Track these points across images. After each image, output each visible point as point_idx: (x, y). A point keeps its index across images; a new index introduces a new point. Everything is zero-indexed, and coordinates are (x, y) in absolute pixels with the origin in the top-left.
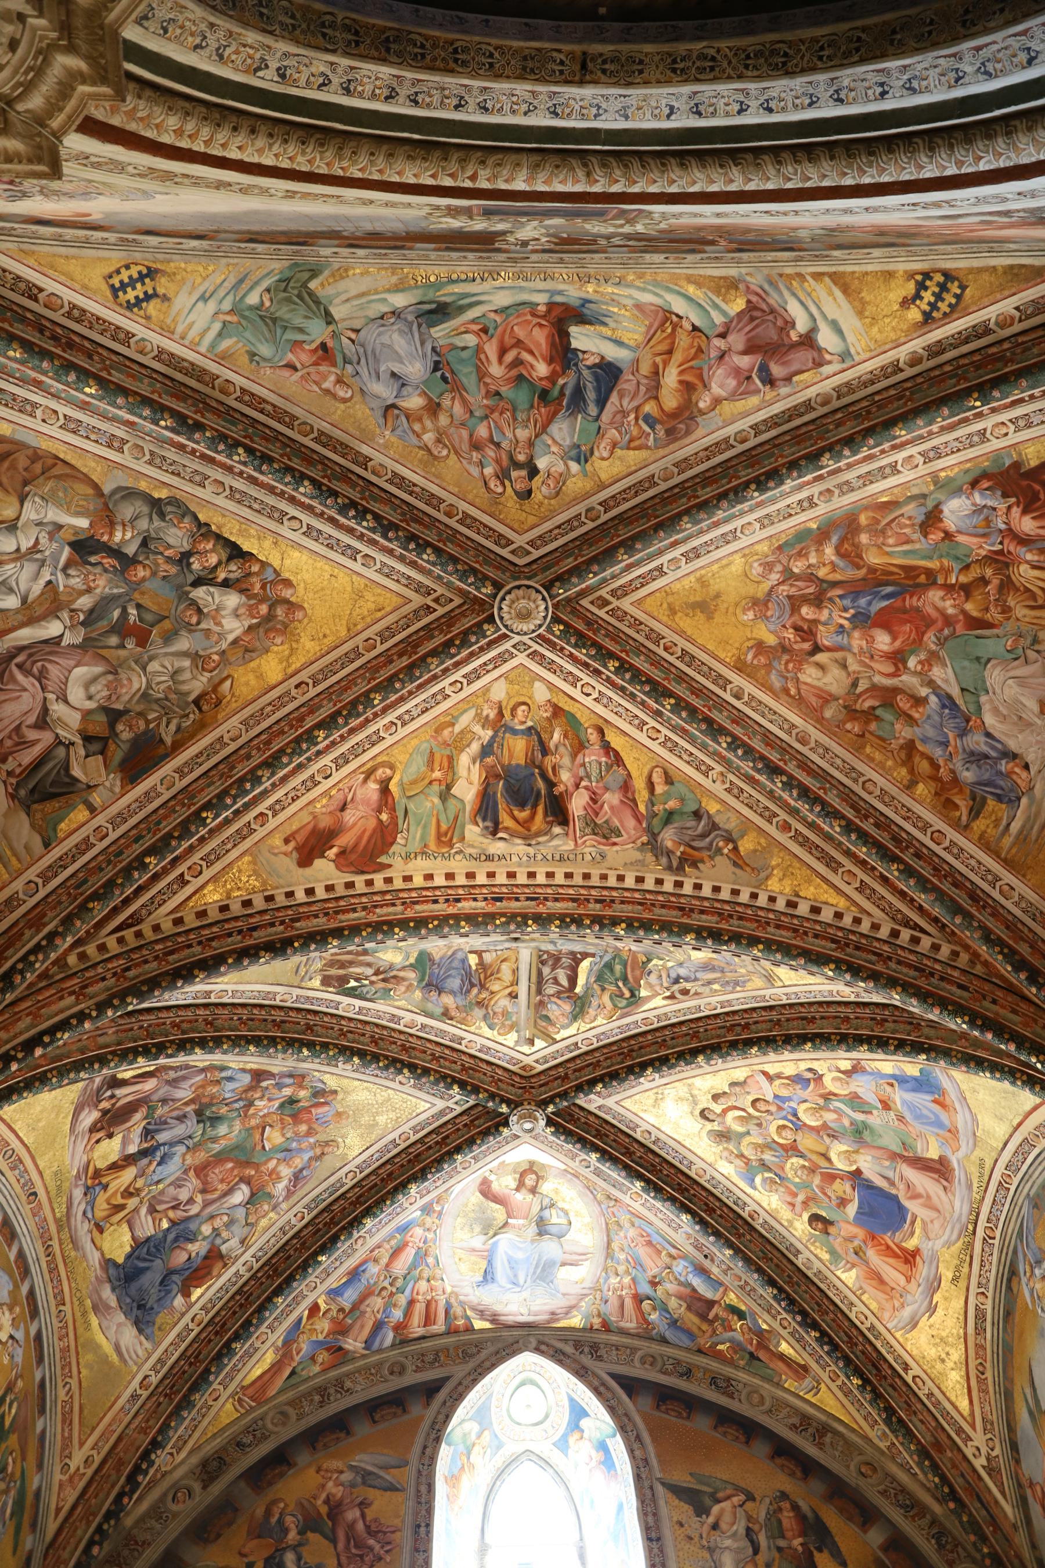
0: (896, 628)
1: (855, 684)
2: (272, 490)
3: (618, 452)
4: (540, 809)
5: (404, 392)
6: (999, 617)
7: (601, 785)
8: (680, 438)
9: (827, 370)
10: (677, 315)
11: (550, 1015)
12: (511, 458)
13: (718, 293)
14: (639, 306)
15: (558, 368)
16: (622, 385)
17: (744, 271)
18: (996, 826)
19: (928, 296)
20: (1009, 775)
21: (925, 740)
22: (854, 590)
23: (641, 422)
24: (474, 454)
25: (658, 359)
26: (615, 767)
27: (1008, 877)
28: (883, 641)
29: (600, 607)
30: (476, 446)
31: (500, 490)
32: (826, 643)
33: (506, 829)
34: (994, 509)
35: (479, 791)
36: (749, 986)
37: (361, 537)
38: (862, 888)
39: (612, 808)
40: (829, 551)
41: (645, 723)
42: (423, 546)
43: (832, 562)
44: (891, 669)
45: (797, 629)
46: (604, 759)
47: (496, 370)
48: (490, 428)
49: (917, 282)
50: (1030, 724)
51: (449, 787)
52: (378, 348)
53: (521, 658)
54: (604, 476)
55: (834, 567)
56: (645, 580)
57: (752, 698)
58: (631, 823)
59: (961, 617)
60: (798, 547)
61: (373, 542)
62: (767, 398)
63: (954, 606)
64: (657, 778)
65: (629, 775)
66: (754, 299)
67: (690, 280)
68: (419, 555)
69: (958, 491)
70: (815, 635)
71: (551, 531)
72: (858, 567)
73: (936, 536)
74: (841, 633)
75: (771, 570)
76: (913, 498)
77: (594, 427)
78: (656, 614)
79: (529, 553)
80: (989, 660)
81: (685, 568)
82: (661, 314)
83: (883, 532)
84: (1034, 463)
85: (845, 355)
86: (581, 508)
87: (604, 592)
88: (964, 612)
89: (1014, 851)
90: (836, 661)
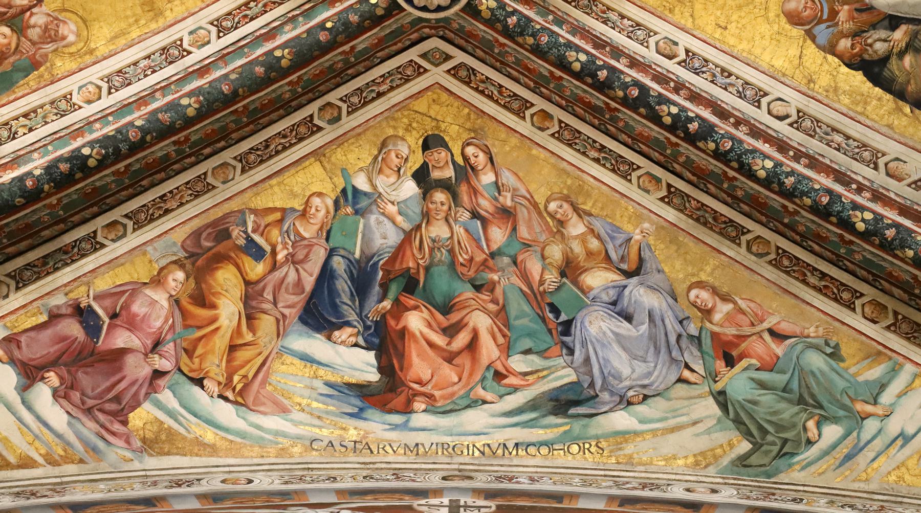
2: (814, 163)
3: (298, 205)
5: (613, 293)
8: (207, 226)
10: (226, 399)
12: (455, 196)
15: (392, 323)
16: (299, 300)
17: (136, 465)
23: (268, 249)
24: (509, 203)
25: (249, 337)
30: (507, 214)
31: (470, 150)
37: (679, 87)
42: (587, 73)
47: (481, 321)
48: (487, 240)
52: (651, 356)
54: (316, 169)
61: (661, 79)
62: (83, 289)
67: (212, 450)
68: (592, 58)
82: (250, 400)
86: (349, 123)
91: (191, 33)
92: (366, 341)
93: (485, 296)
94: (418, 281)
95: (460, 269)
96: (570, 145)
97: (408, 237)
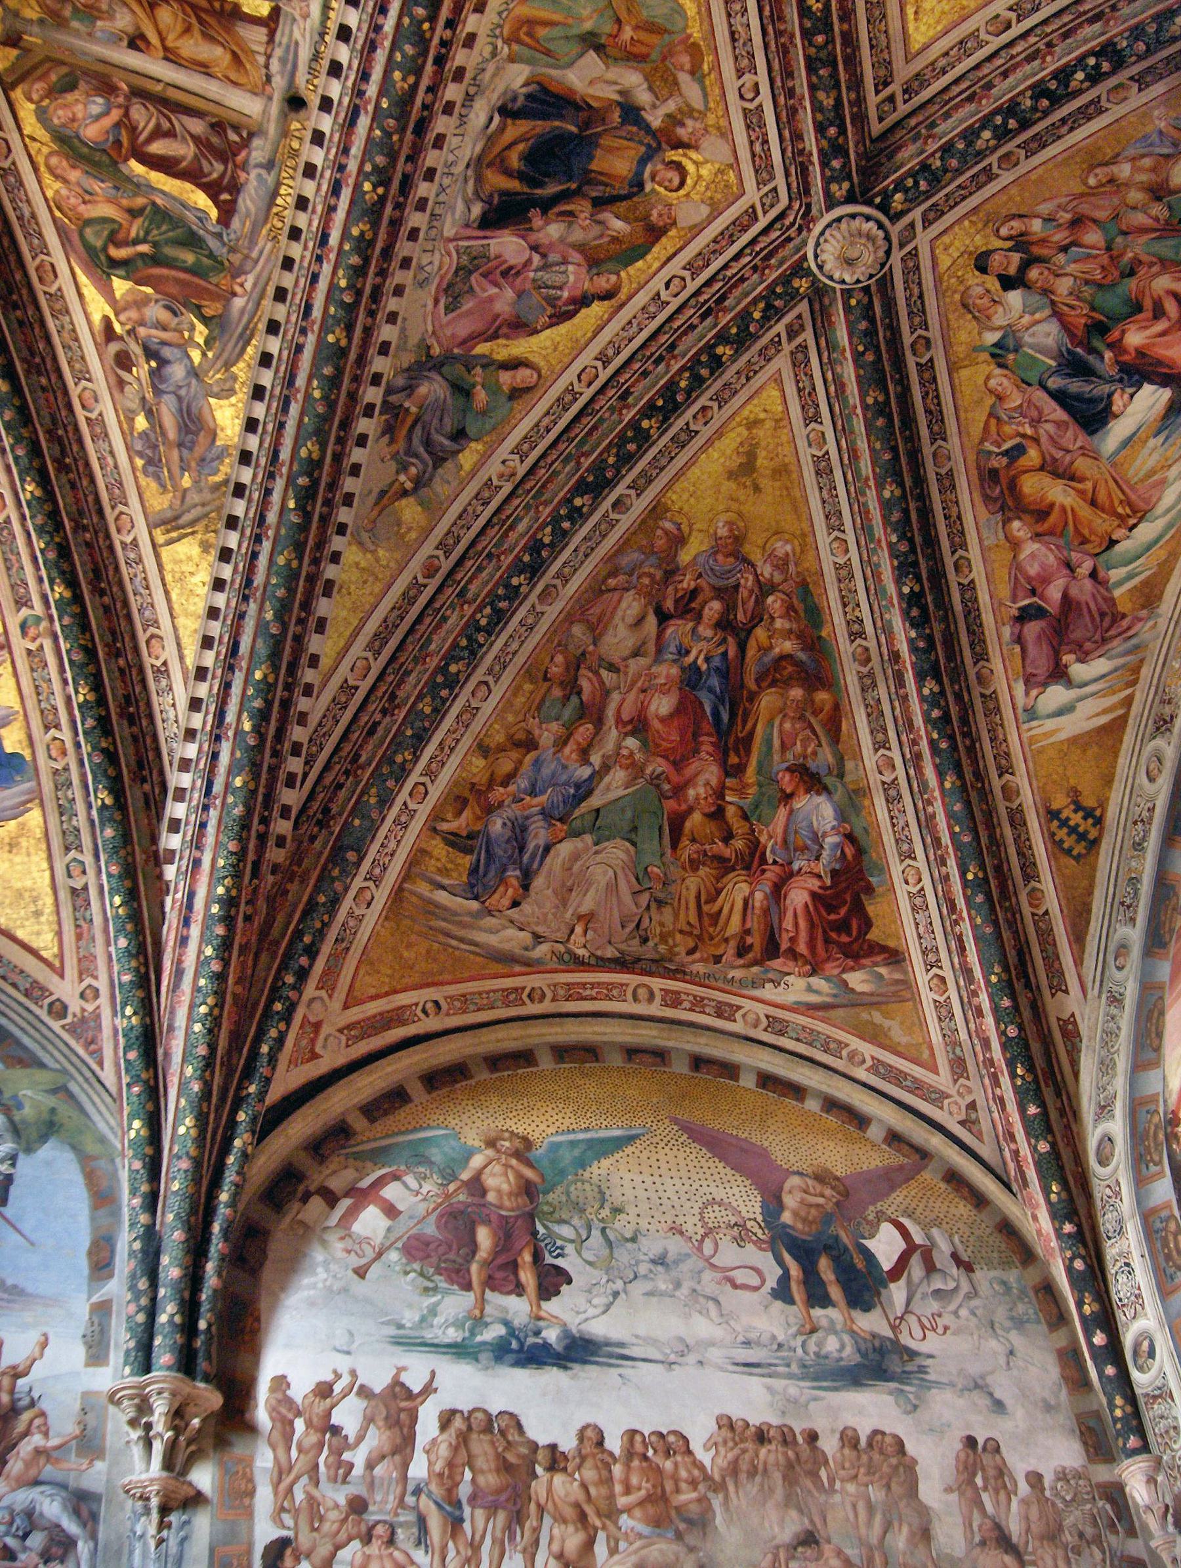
0: (676, 723)
1: (612, 668)
3: (990, 401)
4: (514, 185)
6: (685, 857)
7: (528, 286)
9: (1019, 688)
10: (1135, 526)
11: (76, 95)
12: (1039, 260)
13: (1146, 583)
14: (1163, 483)
15: (1126, 358)
16: (1073, 430)
18: (440, 871)
19: (1076, 818)
20: (502, 880)
21: (537, 763)
22: (729, 672)
23: (1018, 440)
24: (1068, 216)
25: (1088, 485)
26: (550, 311)
27: (382, 896)
28: (662, 705)
29: (789, 327)
30: (1077, 222)
32: (669, 631)
33: (502, 129)
34: (818, 858)
35: (572, 92)
36: (150, 485)
38: (347, 689)
39: (491, 300)
40: (788, 646)
41: (606, 364)
43: (771, 647)
44: (625, 717)
45: (694, 593)
46: (566, 294)
48: (1093, 247)
49: (1094, 809)
50: (564, 903)
51: (599, 49)
53: (752, 195)
54: (964, 373)
55: (764, 650)
56: (807, 396)
57: (612, 525)
58: (463, 329)
59: (684, 807)
60: (799, 606)
63: (697, 798)
64: (524, 376)
65: (536, 332)
66: (1125, 623)
69: (842, 816)
70: (681, 617)
71: (920, 284)
72: (758, 681)
73: (787, 782)
74: (679, 653)
75: (776, 567)
76: (841, 761)
77: (1033, 377)
78: (755, 401)
79: (902, 246)
80: (634, 844)
81: (806, 454)
83: (802, 718)
84: (871, 910)
85: (1031, 713)
86: (934, 333)
87: (808, 336)
88: (690, 810)
89: (414, 899)
90: (644, 643)
91: (810, 445)
92: (1131, 386)
93: (1142, 271)
94: (1101, 322)
95: (1105, 282)
96: (1044, 147)
97: (1057, 314)
